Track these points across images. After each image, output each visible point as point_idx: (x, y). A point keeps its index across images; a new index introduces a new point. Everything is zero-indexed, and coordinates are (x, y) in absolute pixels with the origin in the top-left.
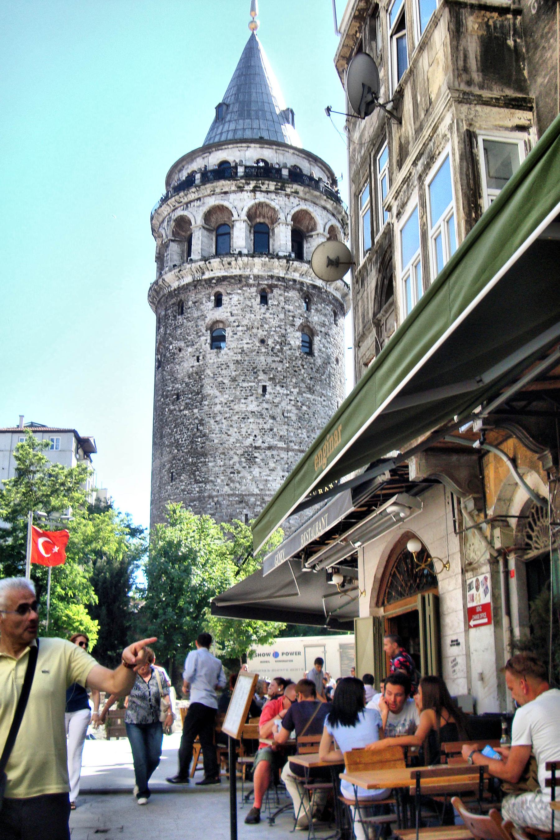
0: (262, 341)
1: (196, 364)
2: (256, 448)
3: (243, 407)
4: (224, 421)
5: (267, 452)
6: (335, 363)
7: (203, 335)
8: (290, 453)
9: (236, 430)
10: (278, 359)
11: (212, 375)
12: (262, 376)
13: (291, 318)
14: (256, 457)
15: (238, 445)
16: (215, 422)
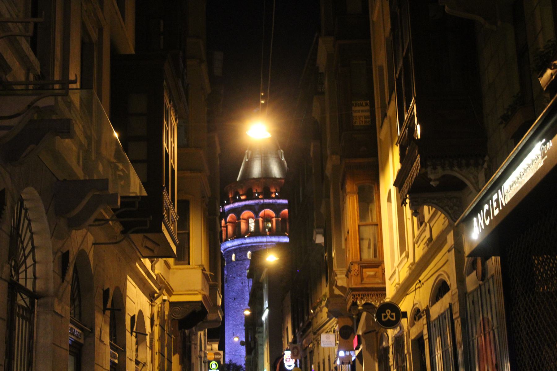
1: (241, 285)
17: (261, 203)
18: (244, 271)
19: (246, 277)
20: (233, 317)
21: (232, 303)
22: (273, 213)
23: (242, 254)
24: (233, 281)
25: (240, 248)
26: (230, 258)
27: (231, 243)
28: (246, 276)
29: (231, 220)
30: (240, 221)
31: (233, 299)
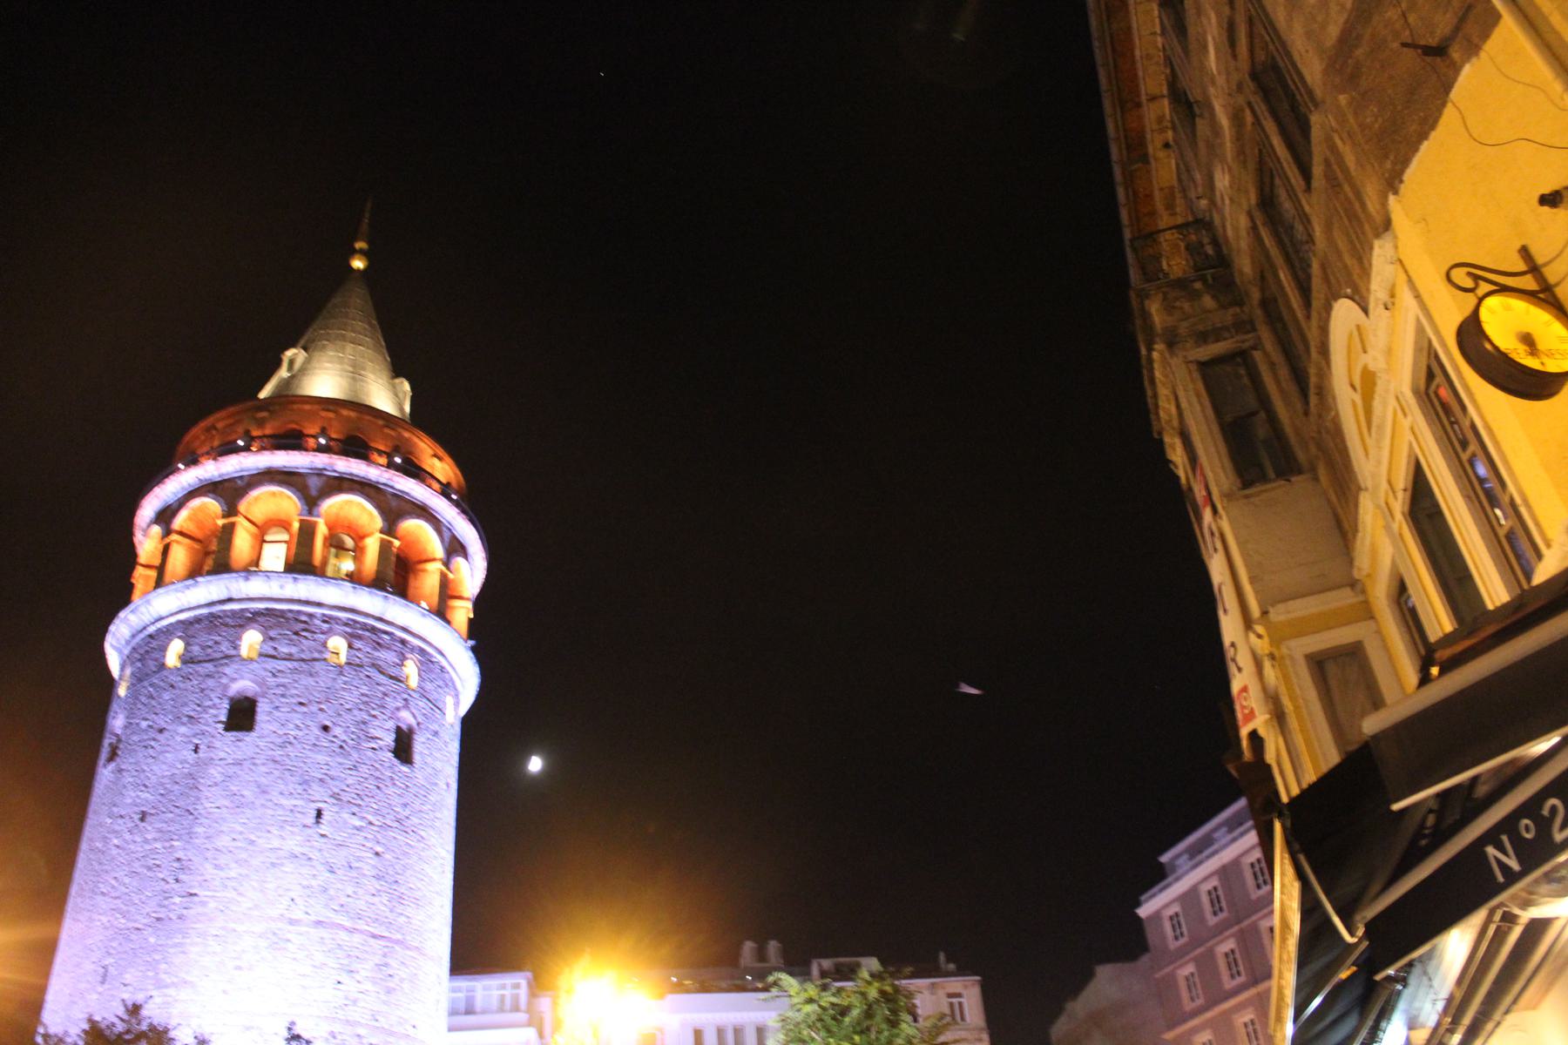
0: (326, 728)
1: (191, 756)
2: (292, 922)
3: (276, 843)
4: (234, 865)
5: (312, 930)
6: (445, 787)
7: (214, 706)
8: (357, 939)
9: (255, 884)
10: (348, 763)
11: (219, 778)
12: (318, 792)
13: (380, 695)
14: (289, 940)
15: (256, 913)
16: (217, 867)
17: (335, 471)
18: (217, 701)
19: (221, 726)
20: (116, 898)
21: (127, 836)
22: (371, 514)
23: (218, 638)
24: (153, 743)
25: (212, 617)
26: (156, 660)
27: (179, 595)
28: (220, 722)
29: (190, 528)
30: (233, 519)
31: (136, 817)
